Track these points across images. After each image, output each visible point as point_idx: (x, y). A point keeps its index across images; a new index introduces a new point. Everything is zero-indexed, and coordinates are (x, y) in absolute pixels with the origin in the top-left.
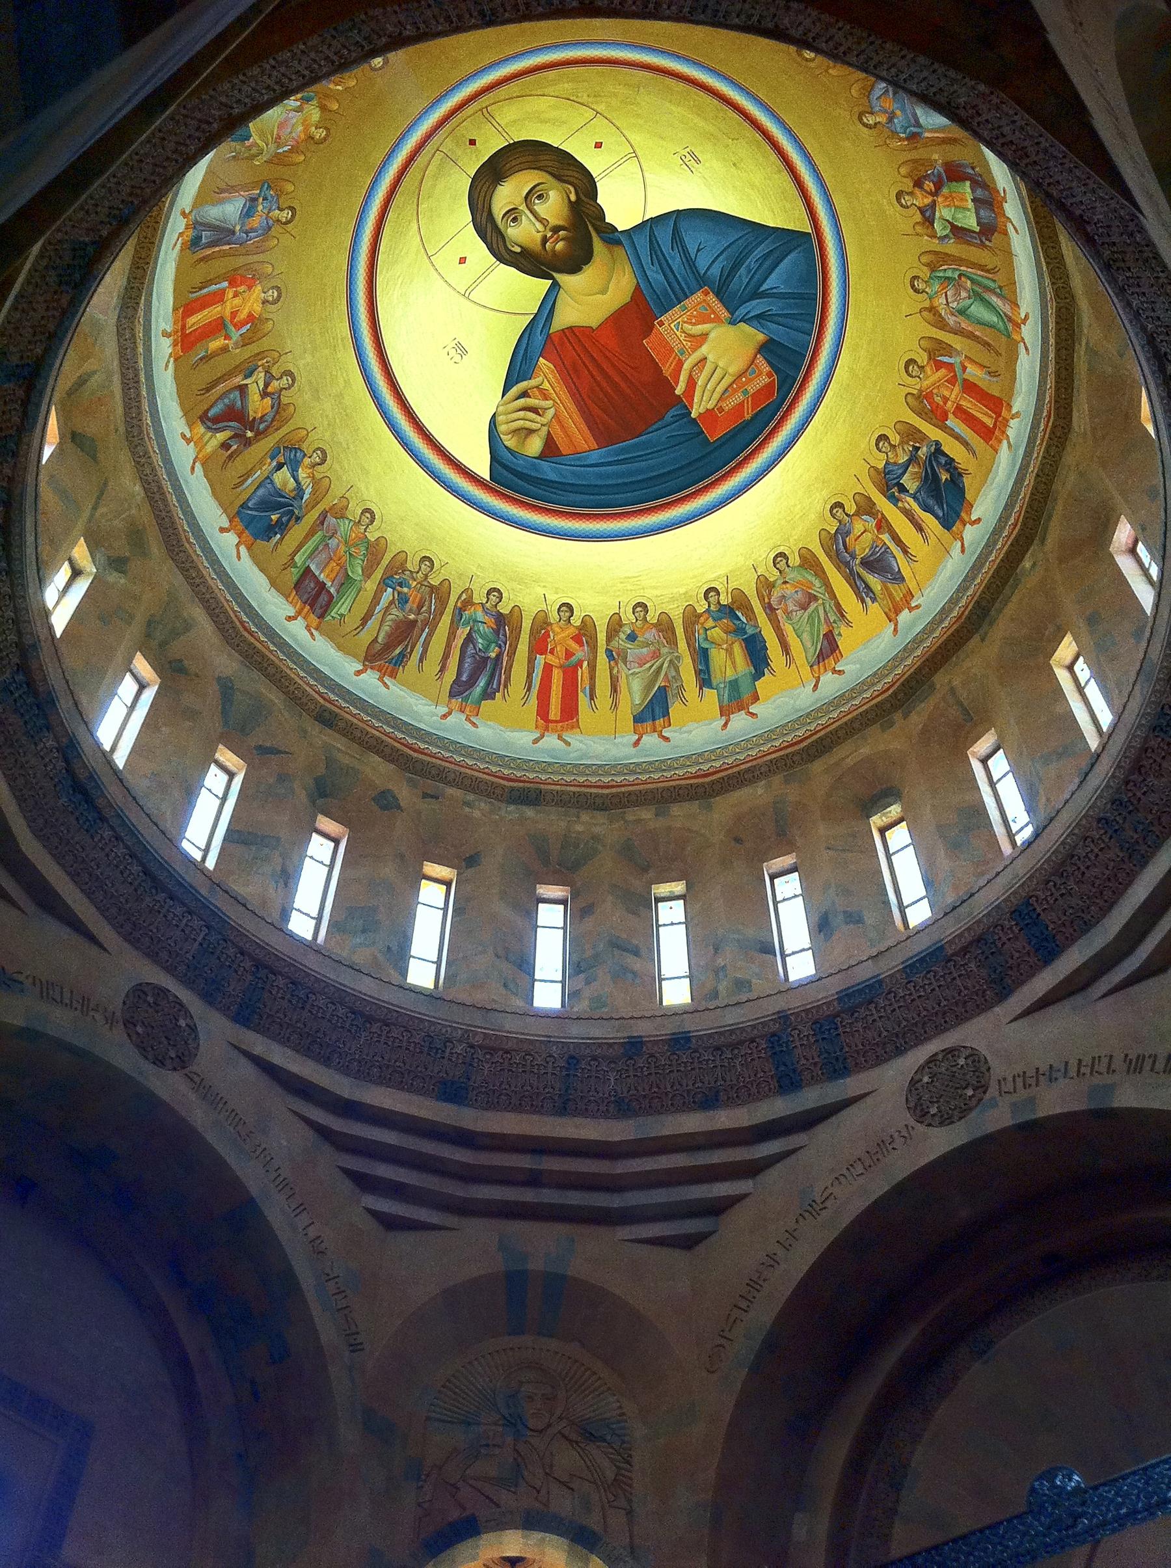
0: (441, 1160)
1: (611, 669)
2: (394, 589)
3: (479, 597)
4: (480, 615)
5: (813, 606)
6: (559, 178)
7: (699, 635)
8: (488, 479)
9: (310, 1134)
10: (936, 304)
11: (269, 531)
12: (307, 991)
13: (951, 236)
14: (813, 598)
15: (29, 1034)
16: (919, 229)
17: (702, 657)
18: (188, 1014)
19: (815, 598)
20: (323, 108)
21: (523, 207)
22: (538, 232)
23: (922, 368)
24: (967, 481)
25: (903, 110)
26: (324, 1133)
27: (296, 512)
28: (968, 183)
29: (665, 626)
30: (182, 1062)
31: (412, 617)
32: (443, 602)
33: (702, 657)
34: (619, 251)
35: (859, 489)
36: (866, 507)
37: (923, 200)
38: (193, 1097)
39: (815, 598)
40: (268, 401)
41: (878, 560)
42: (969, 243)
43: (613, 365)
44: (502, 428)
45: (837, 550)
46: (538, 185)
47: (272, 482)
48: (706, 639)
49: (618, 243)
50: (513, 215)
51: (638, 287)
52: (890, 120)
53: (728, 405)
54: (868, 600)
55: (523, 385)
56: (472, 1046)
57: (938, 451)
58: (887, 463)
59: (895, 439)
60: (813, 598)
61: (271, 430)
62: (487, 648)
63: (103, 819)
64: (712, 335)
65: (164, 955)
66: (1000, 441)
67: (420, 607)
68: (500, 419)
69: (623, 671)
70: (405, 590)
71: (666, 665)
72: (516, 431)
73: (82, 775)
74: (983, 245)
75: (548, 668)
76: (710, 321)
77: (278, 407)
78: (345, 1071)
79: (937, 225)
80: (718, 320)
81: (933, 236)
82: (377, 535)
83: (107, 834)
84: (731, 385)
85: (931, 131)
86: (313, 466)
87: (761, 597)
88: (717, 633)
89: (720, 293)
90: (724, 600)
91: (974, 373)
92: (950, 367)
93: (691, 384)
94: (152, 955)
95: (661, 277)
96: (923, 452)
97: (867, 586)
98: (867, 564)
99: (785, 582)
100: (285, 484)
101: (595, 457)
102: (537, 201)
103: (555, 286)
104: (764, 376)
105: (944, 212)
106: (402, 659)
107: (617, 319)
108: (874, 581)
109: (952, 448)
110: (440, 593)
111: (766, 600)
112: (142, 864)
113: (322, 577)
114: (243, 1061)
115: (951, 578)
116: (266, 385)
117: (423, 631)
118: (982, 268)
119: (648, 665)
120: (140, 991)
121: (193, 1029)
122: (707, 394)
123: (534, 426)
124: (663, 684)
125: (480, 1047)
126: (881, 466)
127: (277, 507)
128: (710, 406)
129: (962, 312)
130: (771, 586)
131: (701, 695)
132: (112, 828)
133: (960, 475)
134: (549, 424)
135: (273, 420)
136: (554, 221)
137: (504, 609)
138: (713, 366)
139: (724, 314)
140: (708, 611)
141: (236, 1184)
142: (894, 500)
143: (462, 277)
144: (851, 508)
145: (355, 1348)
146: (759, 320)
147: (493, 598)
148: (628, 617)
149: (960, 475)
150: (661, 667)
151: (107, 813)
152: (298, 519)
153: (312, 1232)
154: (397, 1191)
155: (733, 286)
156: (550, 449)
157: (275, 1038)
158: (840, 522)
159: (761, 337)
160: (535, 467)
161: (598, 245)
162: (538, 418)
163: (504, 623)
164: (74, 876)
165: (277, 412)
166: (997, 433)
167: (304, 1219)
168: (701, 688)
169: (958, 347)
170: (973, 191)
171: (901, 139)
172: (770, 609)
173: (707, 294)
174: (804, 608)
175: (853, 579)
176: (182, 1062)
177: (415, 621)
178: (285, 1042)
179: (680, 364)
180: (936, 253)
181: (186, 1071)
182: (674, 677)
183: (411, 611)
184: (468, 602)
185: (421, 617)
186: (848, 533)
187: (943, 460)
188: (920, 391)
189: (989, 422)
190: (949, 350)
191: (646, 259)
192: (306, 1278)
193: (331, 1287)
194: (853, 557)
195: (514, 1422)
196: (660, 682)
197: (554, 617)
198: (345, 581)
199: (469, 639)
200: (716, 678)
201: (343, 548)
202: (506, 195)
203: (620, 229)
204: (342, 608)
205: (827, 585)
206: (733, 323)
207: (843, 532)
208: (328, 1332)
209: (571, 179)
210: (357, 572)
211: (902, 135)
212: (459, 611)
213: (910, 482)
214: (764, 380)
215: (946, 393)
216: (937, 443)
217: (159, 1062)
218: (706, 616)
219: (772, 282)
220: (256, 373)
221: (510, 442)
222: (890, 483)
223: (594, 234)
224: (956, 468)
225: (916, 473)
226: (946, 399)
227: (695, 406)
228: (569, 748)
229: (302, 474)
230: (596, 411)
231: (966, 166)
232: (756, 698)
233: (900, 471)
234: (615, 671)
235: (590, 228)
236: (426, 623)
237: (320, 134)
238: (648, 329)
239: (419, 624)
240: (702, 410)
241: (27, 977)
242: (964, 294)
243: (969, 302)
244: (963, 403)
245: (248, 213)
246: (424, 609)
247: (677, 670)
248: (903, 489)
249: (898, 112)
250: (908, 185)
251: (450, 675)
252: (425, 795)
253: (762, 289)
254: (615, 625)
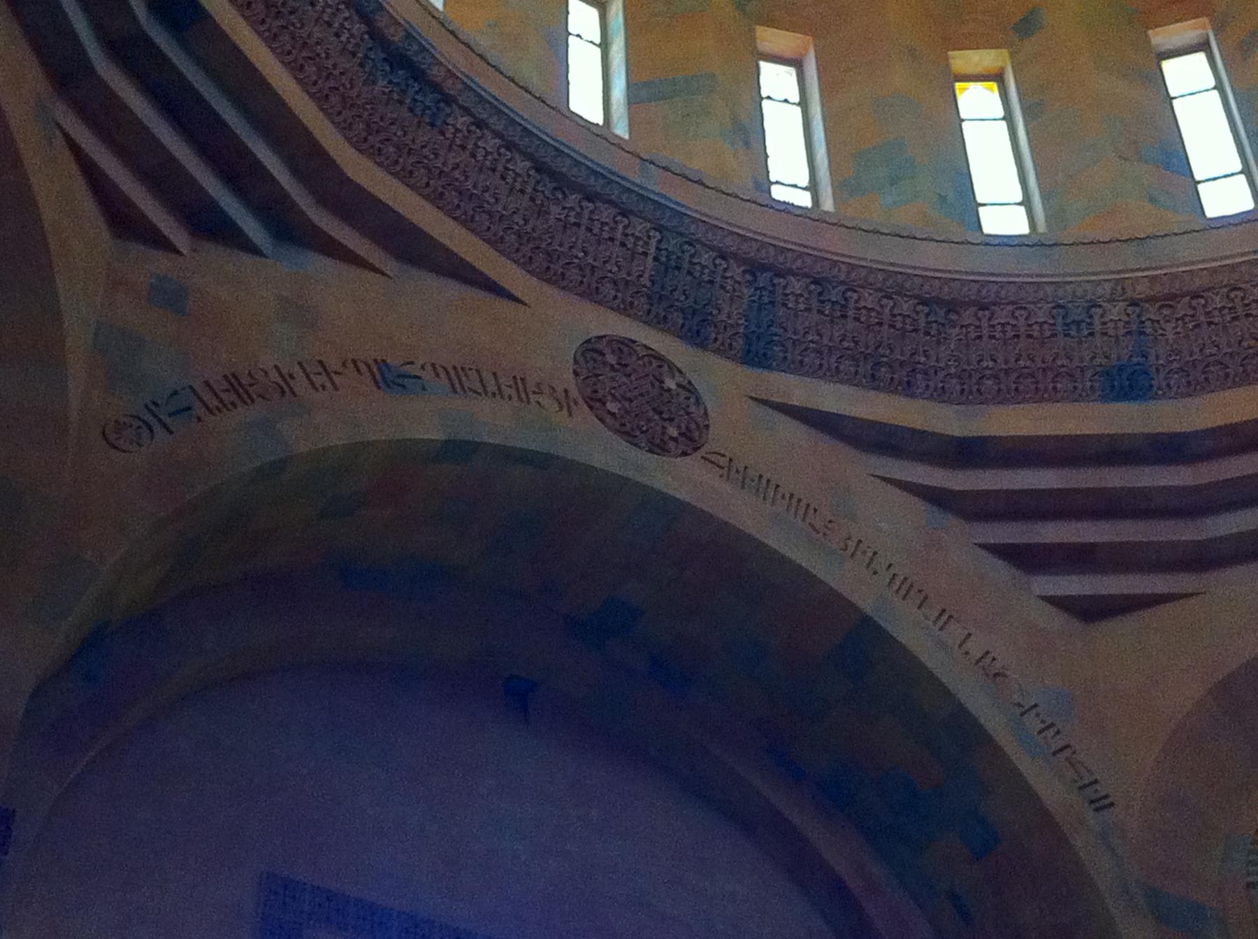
12: (842, 288)
18: (674, 369)
30: (691, 441)
38: (726, 487)
56: (1134, 303)
63: (449, 100)
65: (608, 289)
73: (397, 37)
78: (941, 395)
83: (462, 121)
94: (591, 294)
112: (529, 157)
114: (782, 420)
120: (591, 349)
125: (1151, 300)
132: (466, 111)
141: (834, 600)
145: (1101, 804)
151: (450, 87)
153: (976, 650)
157: (819, 372)
164: (436, 199)
167: (955, 632)
176: (691, 441)
178: (835, 375)
181: (702, 452)
192: (993, 721)
217: (658, 447)
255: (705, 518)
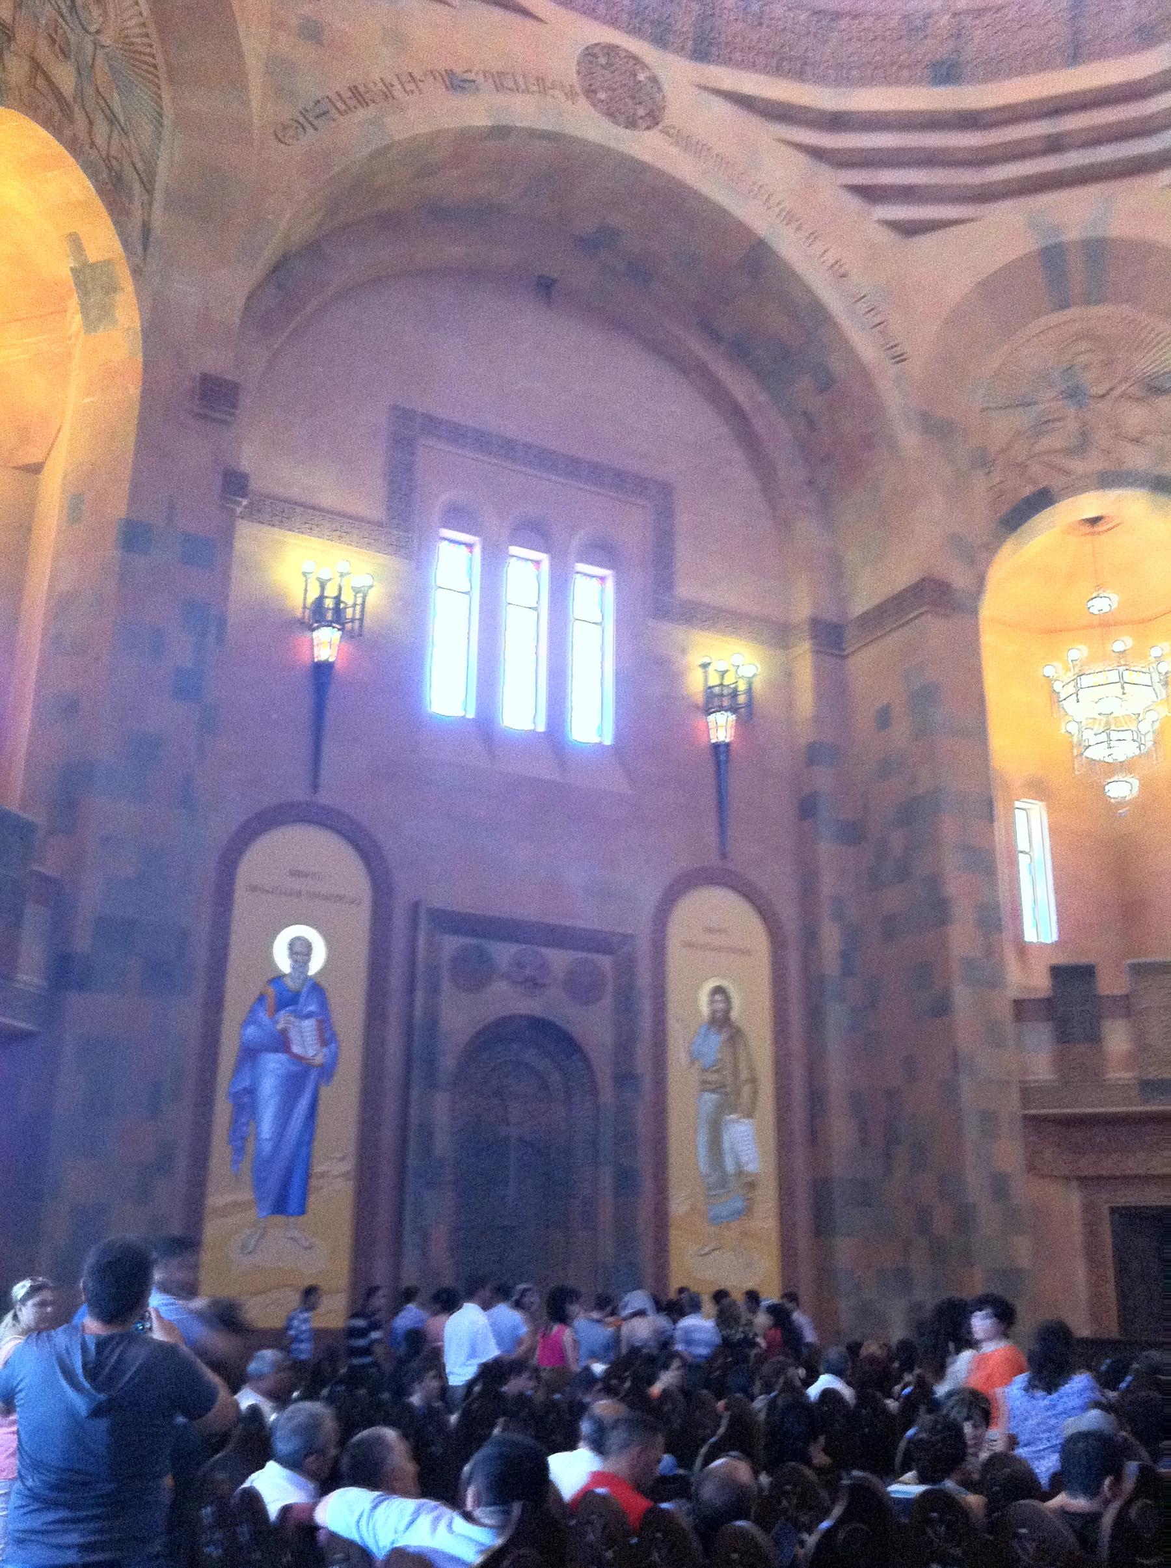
0: (945, 150)
9: (801, 158)
15: (500, 132)
18: (645, 66)
26: (817, 154)
30: (654, 118)
38: (674, 150)
120: (590, 53)
121: (654, 80)
141: (742, 229)
145: (900, 359)
154: (907, 194)
157: (741, 65)
167: (819, 247)
176: (654, 118)
178: (753, 67)
181: (660, 127)
193: (862, 307)
195: (1074, 394)
208: (867, 349)
217: (631, 124)
241: (477, 73)
255: (660, 173)
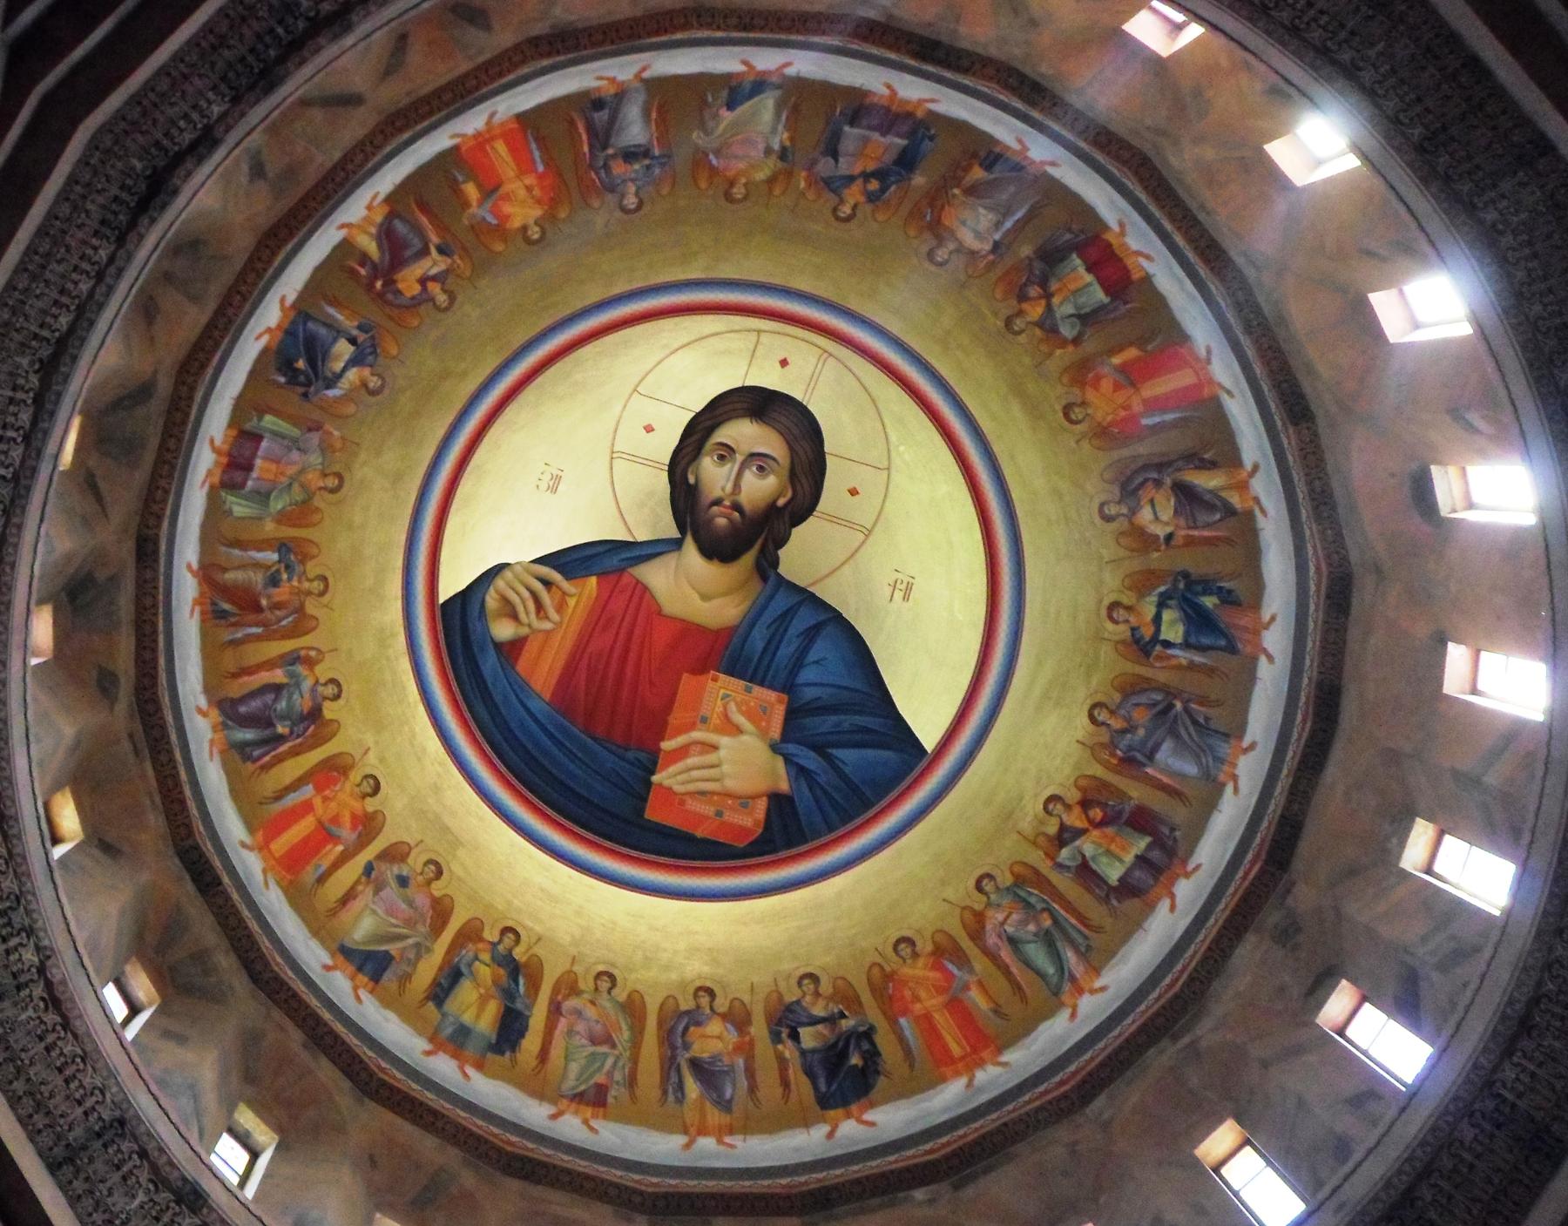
1: (357, 882)
2: (280, 561)
3: (323, 671)
4: (307, 685)
5: (604, 1049)
6: (793, 476)
7: (468, 952)
8: (441, 600)
10: (990, 913)
11: (287, 366)
13: (1073, 870)
14: (608, 1040)
16: (1041, 840)
17: (451, 978)
19: (614, 1046)
20: (771, 181)
21: (739, 458)
22: (723, 489)
23: (915, 955)
24: (882, 1082)
25: (1149, 734)
27: (312, 389)
28: (1148, 839)
29: (441, 912)
31: (264, 602)
32: (295, 632)
33: (451, 978)
34: (756, 586)
35: (746, 998)
36: (738, 1018)
37: (1075, 819)
39: (614, 1046)
40: (417, 288)
41: (713, 1073)
42: (1089, 890)
43: (640, 658)
44: (500, 583)
45: (671, 1031)
46: (774, 459)
47: (335, 340)
48: (470, 965)
49: (764, 578)
50: (726, 453)
51: (737, 627)
52: (1124, 731)
53: (694, 806)
54: (671, 1098)
55: (556, 576)
57: (868, 1034)
58: (798, 1002)
59: (826, 987)
60: (608, 1040)
61: (387, 310)
62: (282, 718)
64: (745, 738)
66: (958, 1074)
67: (277, 606)
68: (508, 574)
69: (366, 895)
70: (285, 576)
71: (411, 941)
72: (505, 600)
74: (1107, 900)
75: (307, 807)
76: (758, 727)
77: (416, 303)
79: (1065, 853)
80: (763, 733)
81: (1051, 856)
82: (322, 505)
84: (713, 793)
85: (1162, 771)
86: (364, 385)
87: (556, 990)
88: (485, 972)
89: (792, 715)
90: (519, 953)
91: (976, 997)
92: (950, 976)
93: (682, 752)
95: (760, 645)
96: (846, 1024)
97: (680, 1087)
98: (695, 1064)
99: (593, 1003)
100: (337, 358)
101: (535, 705)
102: (754, 469)
103: (676, 544)
104: (752, 819)
105: (1088, 846)
106: (221, 615)
107: (688, 631)
108: (692, 1088)
109: (885, 1041)
110: (302, 624)
111: (560, 997)
113: (258, 462)
115: (796, 1150)
116: (434, 278)
117: (257, 625)
118: (1082, 919)
119: (393, 921)
122: (684, 777)
123: (522, 616)
124: (393, 953)
126: (790, 997)
127: (312, 362)
128: (678, 788)
129: (1013, 941)
130: (574, 990)
131: (422, 1003)
133: (878, 1073)
134: (534, 631)
135: (399, 307)
136: (744, 498)
137: (330, 711)
138: (716, 762)
139: (776, 732)
140: (494, 945)
142: (776, 1038)
143: (631, 439)
144: (722, 1004)
146: (798, 771)
147: (330, 690)
148: (416, 861)
149: (878, 1073)
150: (406, 937)
152: (305, 395)
155: (807, 721)
156: (509, 651)
158: (698, 1007)
159: (784, 786)
160: (482, 649)
161: (748, 559)
162: (533, 616)
163: (313, 722)
165: (407, 307)
166: (960, 1065)
168: (427, 998)
169: (978, 967)
170: (1149, 847)
171: (1113, 755)
172: (555, 1010)
173: (780, 702)
174: (594, 1041)
175: (669, 1065)
177: (258, 609)
179: (692, 727)
180: (1036, 872)
182: (409, 960)
183: (269, 597)
184: (310, 663)
185: (268, 615)
186: (698, 1024)
187: (866, 1046)
188: (894, 972)
189: (956, 1050)
190: (962, 959)
191: (768, 617)
194: (687, 1047)
196: (393, 948)
197: (355, 776)
198: (262, 497)
199: (277, 689)
200: (451, 1005)
201: (291, 471)
202: (743, 433)
203: (782, 570)
204: (239, 508)
205: (636, 1044)
206: (775, 748)
207: (694, 1018)
209: (799, 488)
210: (277, 504)
211: (1119, 752)
212: (293, 659)
213: (809, 1037)
214: (746, 821)
215: (923, 994)
216: (872, 1029)
218: (489, 947)
219: (846, 755)
220: (445, 258)
221: (492, 601)
222: (786, 1020)
223: (757, 547)
224: (875, 1063)
225: (821, 1034)
226: (917, 999)
227: (664, 774)
228: (264, 890)
229: (353, 375)
230: (582, 675)
231: (1163, 822)
232: (479, 1066)
233: (805, 1020)
234: (360, 888)
235: (763, 536)
236: (264, 624)
237: (738, 191)
238: (700, 669)
239: (261, 617)
240: (667, 783)
242: (1032, 927)
243: (1031, 938)
244: (936, 1016)
245: (630, 155)
246: (278, 613)
247: (419, 957)
248: (795, 1036)
249: (1141, 732)
250: (1073, 796)
251: (236, 689)
252: (131, 736)
253: (834, 751)
254: (396, 854)
